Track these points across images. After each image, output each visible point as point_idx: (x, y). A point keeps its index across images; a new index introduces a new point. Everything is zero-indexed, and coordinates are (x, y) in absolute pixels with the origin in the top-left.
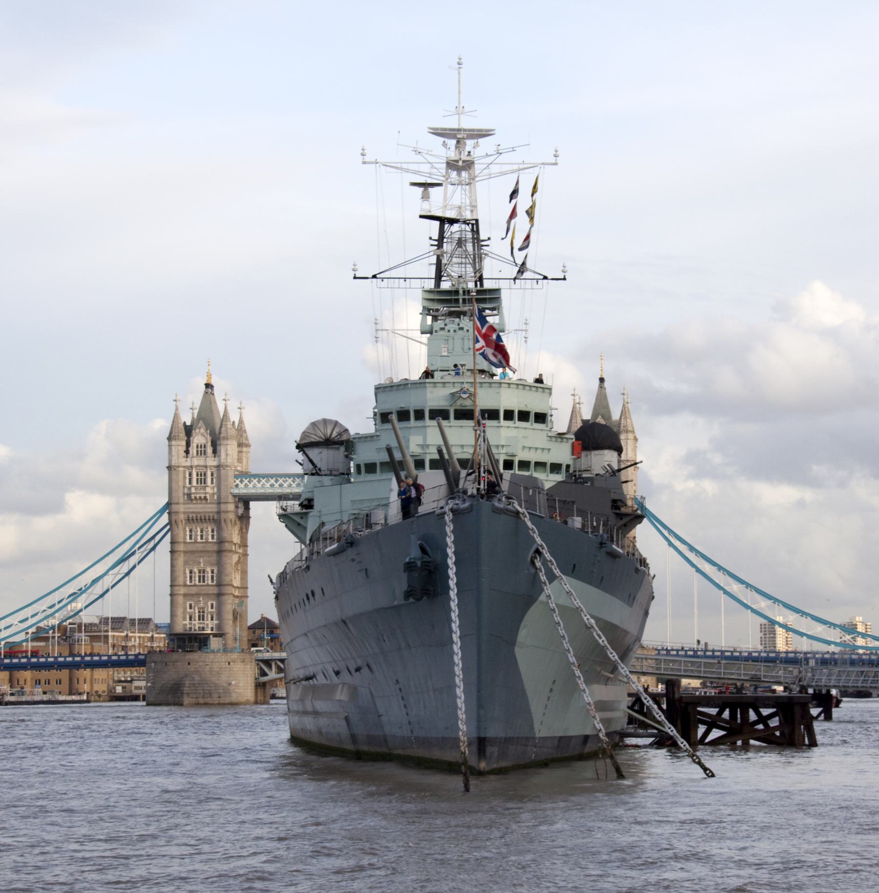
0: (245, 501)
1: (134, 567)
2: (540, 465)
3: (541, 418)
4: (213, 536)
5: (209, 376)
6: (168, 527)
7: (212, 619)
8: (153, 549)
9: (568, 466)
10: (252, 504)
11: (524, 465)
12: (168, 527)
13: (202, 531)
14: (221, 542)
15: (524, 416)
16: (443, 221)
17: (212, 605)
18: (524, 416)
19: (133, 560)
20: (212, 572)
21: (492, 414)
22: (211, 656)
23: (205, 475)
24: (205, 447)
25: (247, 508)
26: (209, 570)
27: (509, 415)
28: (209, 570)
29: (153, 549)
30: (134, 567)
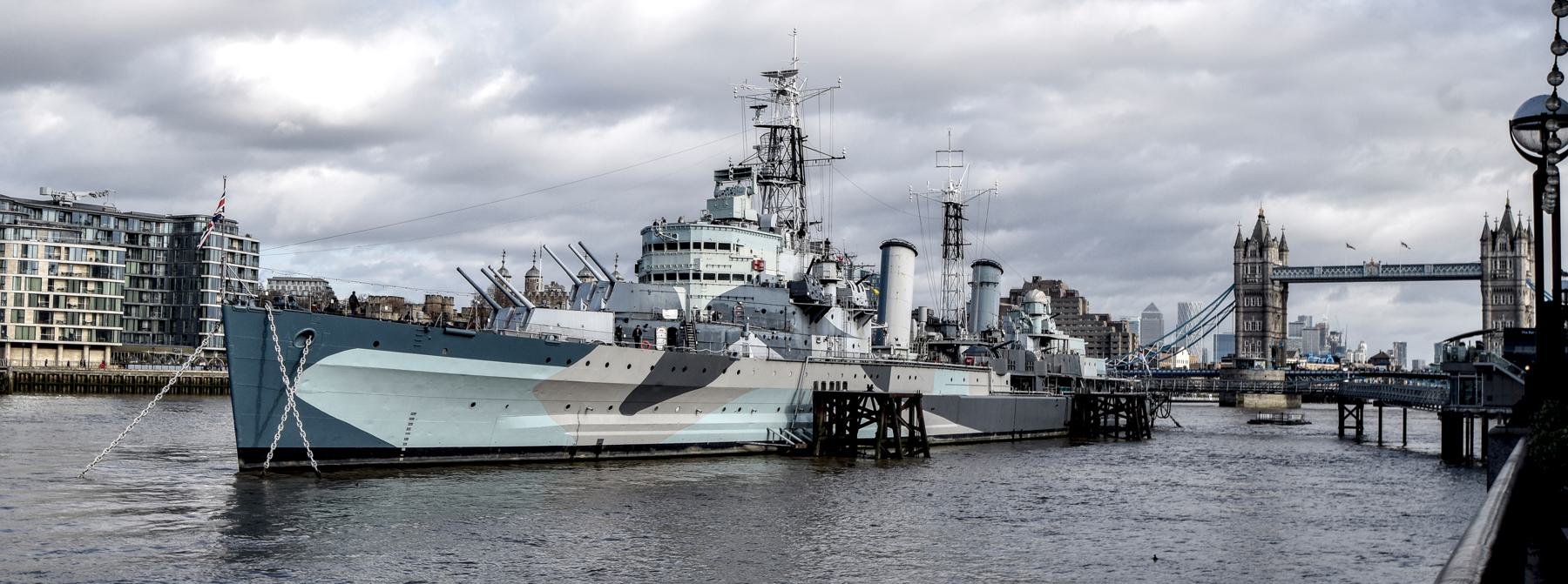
0: (1285, 283)
2: (724, 277)
9: (750, 277)
11: (710, 277)
14: (1265, 306)
15: (710, 246)
16: (776, 127)
18: (710, 246)
21: (685, 246)
25: (1286, 287)
27: (697, 246)
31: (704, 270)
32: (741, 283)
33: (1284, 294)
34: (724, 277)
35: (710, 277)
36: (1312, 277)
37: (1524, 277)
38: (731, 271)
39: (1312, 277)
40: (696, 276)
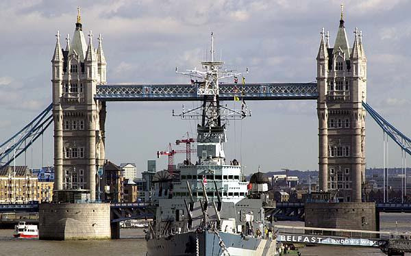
1: (30, 144)
2: (236, 194)
3: (237, 177)
4: (82, 126)
5: (79, 19)
6: (52, 118)
7: (82, 181)
8: (42, 133)
10: (107, 102)
11: (231, 194)
12: (52, 118)
13: (75, 123)
15: (231, 177)
17: (82, 172)
19: (29, 140)
20: (82, 150)
21: (219, 177)
22: (82, 206)
23: (77, 85)
24: (77, 67)
25: (104, 106)
26: (79, 148)
27: (225, 177)
28: (79, 148)
29: (42, 133)
30: (30, 144)
31: (229, 191)
32: (243, 197)
33: (103, 114)
34: (236, 194)
35: (231, 194)
36: (135, 94)
37: (360, 100)
38: (239, 191)
39: (135, 94)
40: (225, 194)
